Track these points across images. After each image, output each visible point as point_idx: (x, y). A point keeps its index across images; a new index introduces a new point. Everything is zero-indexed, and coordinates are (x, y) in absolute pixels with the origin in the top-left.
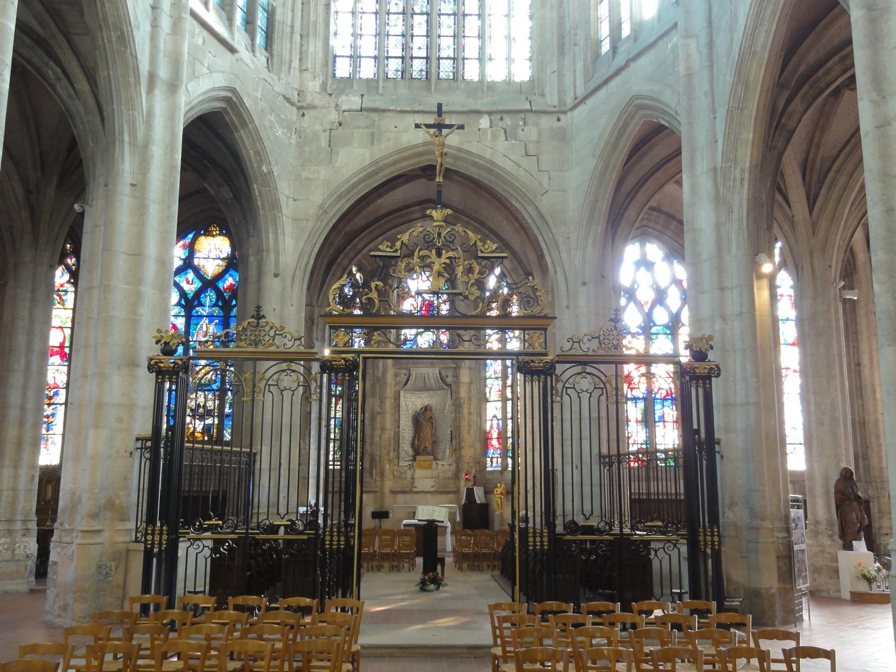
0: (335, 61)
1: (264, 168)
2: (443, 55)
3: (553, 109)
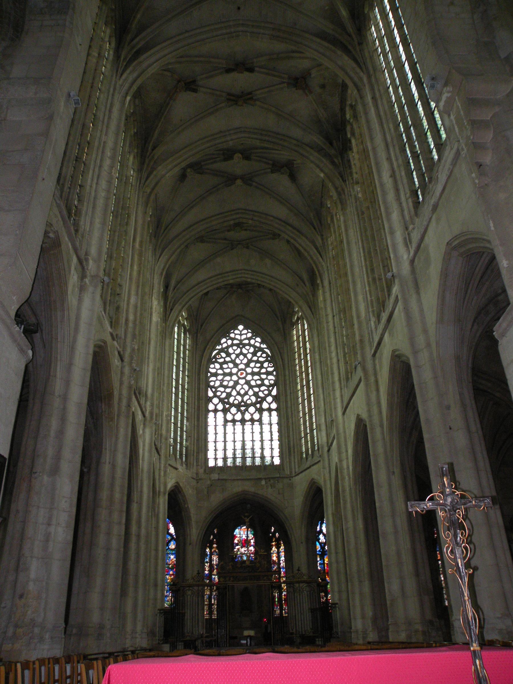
1: (186, 506)
2: (247, 456)
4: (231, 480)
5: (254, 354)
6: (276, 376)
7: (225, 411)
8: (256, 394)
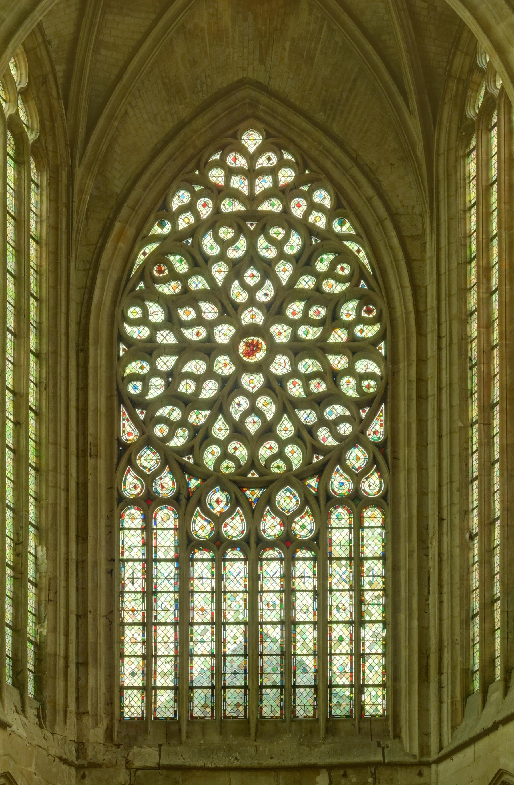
0: (122, 696)
2: (266, 682)
3: (412, 760)
4: (204, 768)
5: (304, 262)
6: (391, 362)
7: (185, 503)
8: (304, 436)
